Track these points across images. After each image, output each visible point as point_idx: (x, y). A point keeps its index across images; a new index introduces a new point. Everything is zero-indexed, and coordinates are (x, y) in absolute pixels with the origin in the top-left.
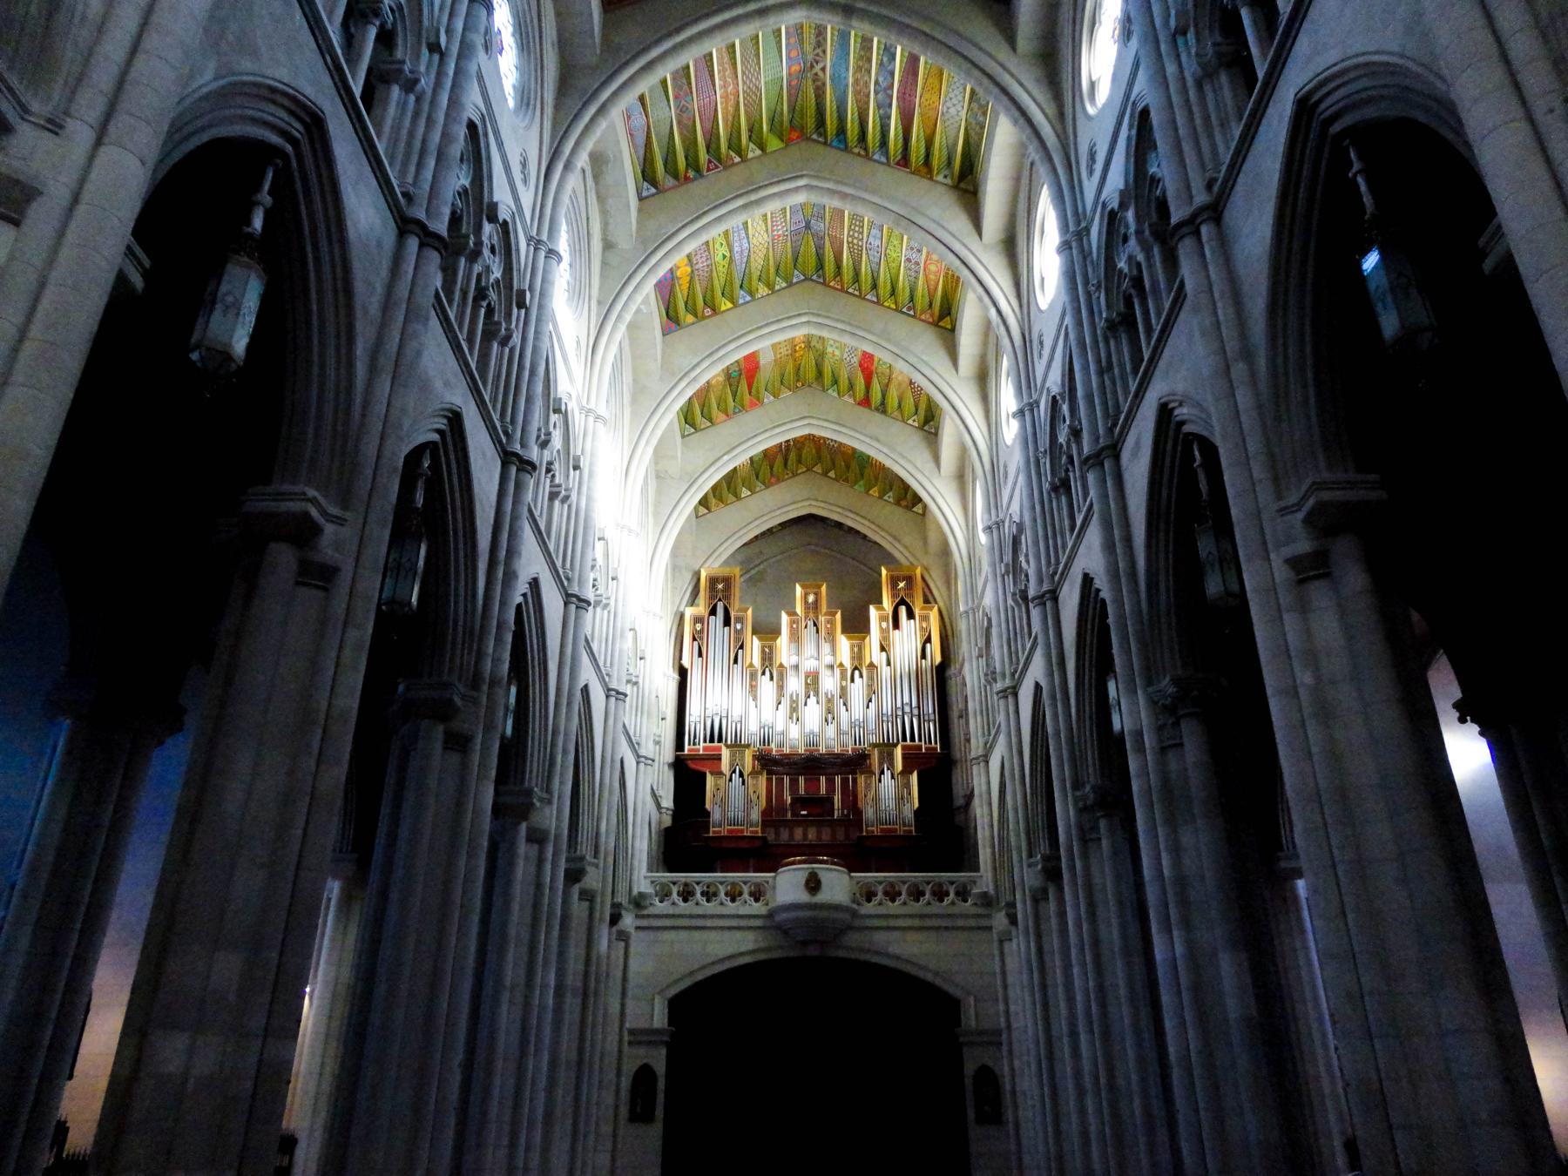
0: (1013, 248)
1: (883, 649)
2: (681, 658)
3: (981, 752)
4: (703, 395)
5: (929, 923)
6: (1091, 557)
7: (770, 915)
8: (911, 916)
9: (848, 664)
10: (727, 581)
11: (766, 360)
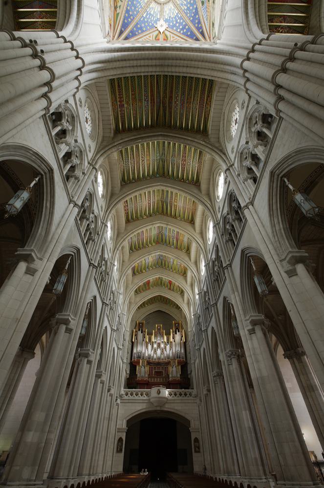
0: (197, 263)
1: (173, 338)
2: (132, 340)
3: (194, 361)
4: (139, 288)
5: (183, 401)
6: (213, 323)
7: (149, 400)
8: (179, 400)
9: (166, 341)
10: (142, 324)
11: (151, 281)
